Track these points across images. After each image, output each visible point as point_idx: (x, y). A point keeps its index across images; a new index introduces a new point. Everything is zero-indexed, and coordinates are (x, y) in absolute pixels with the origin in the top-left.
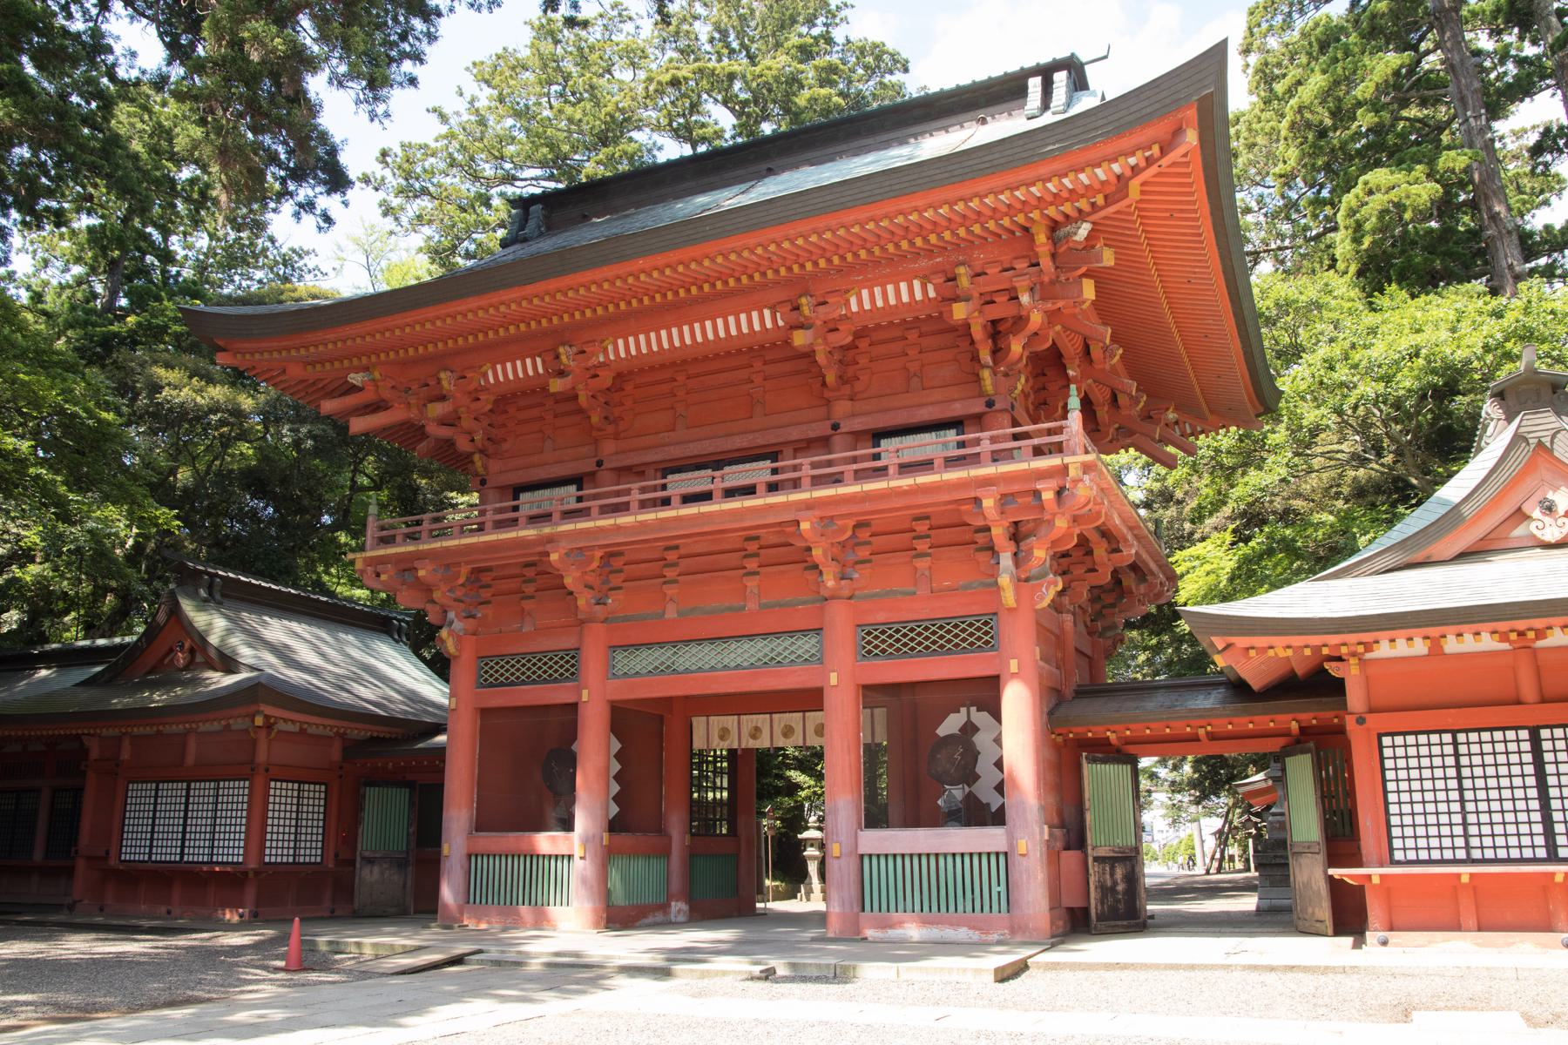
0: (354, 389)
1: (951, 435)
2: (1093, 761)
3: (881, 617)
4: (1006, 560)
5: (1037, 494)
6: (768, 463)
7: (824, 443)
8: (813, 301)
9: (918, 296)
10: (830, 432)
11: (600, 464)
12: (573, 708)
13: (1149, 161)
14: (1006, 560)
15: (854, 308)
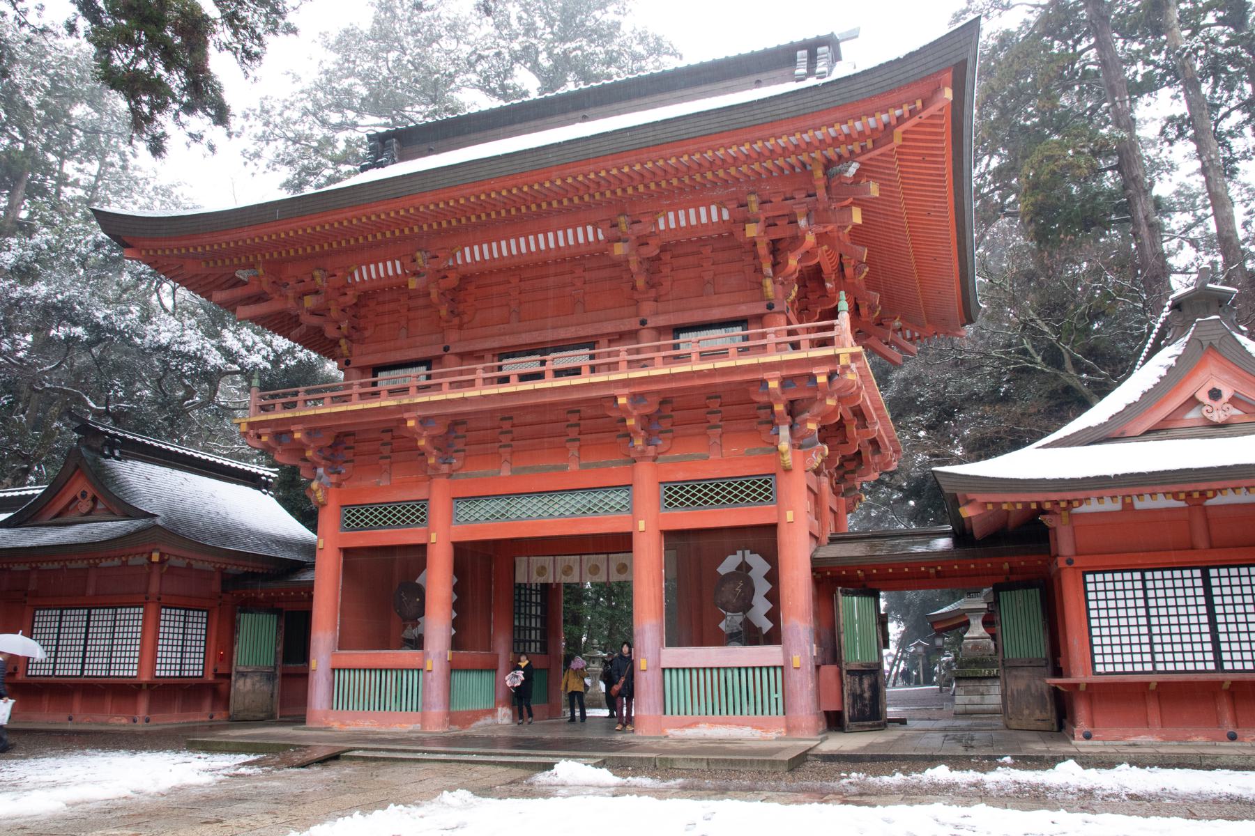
0: (238, 283)
1: (738, 331)
2: (846, 594)
3: (681, 476)
5: (812, 377)
6: (587, 351)
7: (631, 335)
8: (629, 220)
9: (715, 218)
10: (639, 326)
11: (446, 349)
12: (422, 548)
13: (912, 113)
14: (784, 432)
15: (662, 227)
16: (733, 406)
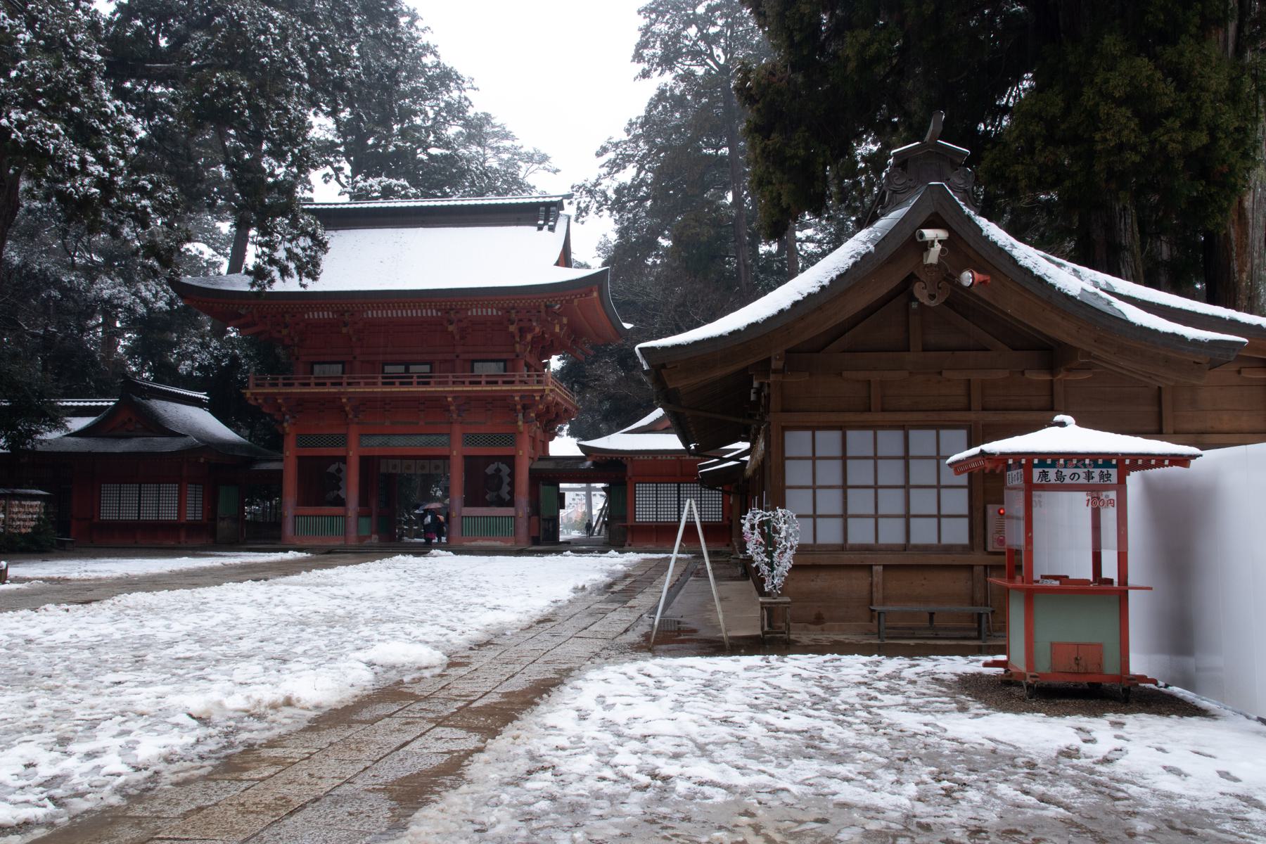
4: (520, 416)
14: (520, 416)
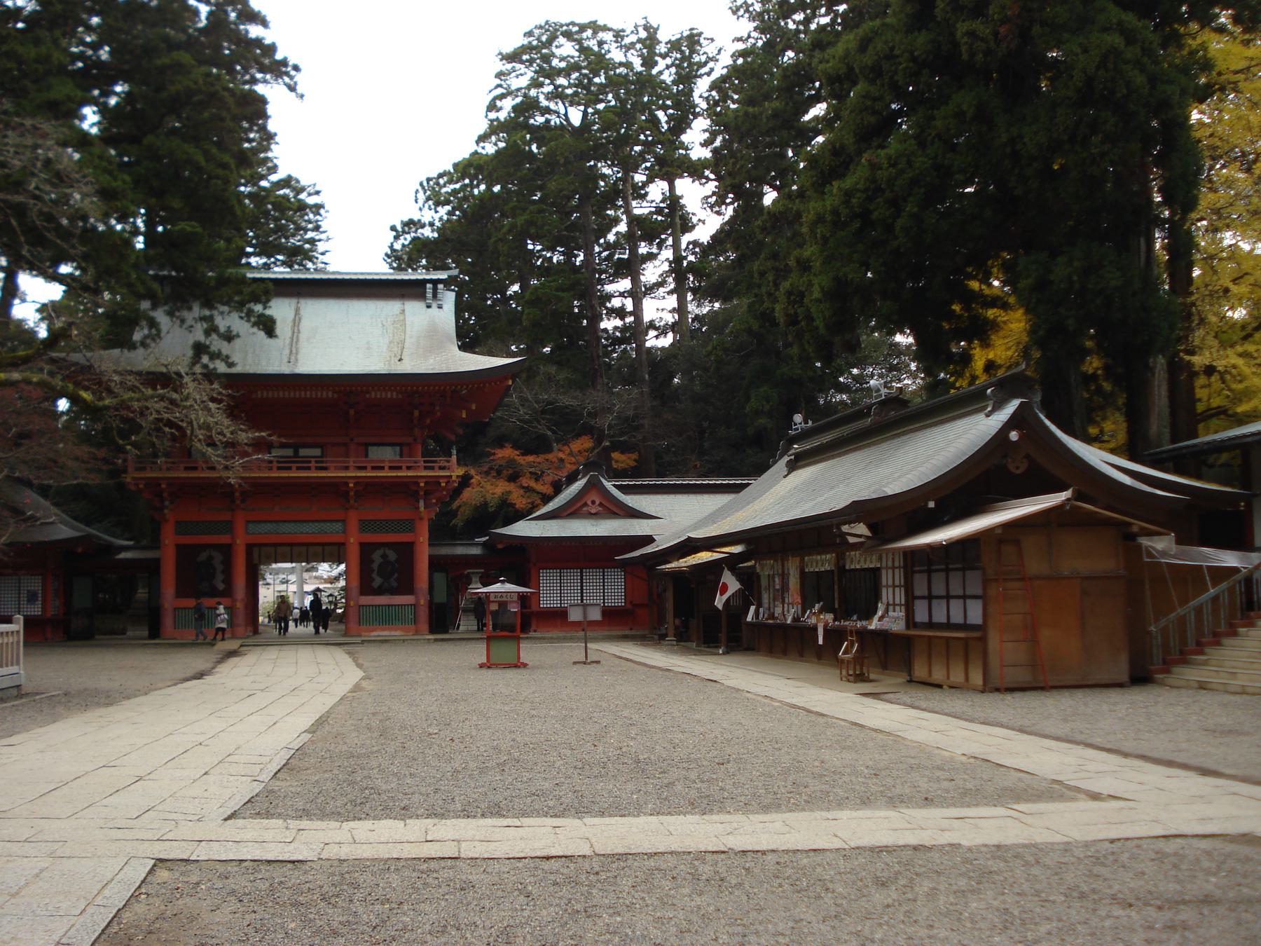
4: (422, 503)
14: (422, 503)
16: (405, 491)
